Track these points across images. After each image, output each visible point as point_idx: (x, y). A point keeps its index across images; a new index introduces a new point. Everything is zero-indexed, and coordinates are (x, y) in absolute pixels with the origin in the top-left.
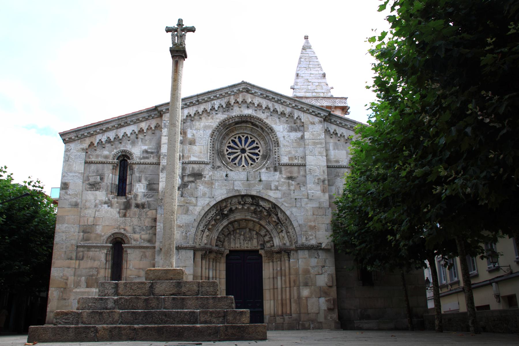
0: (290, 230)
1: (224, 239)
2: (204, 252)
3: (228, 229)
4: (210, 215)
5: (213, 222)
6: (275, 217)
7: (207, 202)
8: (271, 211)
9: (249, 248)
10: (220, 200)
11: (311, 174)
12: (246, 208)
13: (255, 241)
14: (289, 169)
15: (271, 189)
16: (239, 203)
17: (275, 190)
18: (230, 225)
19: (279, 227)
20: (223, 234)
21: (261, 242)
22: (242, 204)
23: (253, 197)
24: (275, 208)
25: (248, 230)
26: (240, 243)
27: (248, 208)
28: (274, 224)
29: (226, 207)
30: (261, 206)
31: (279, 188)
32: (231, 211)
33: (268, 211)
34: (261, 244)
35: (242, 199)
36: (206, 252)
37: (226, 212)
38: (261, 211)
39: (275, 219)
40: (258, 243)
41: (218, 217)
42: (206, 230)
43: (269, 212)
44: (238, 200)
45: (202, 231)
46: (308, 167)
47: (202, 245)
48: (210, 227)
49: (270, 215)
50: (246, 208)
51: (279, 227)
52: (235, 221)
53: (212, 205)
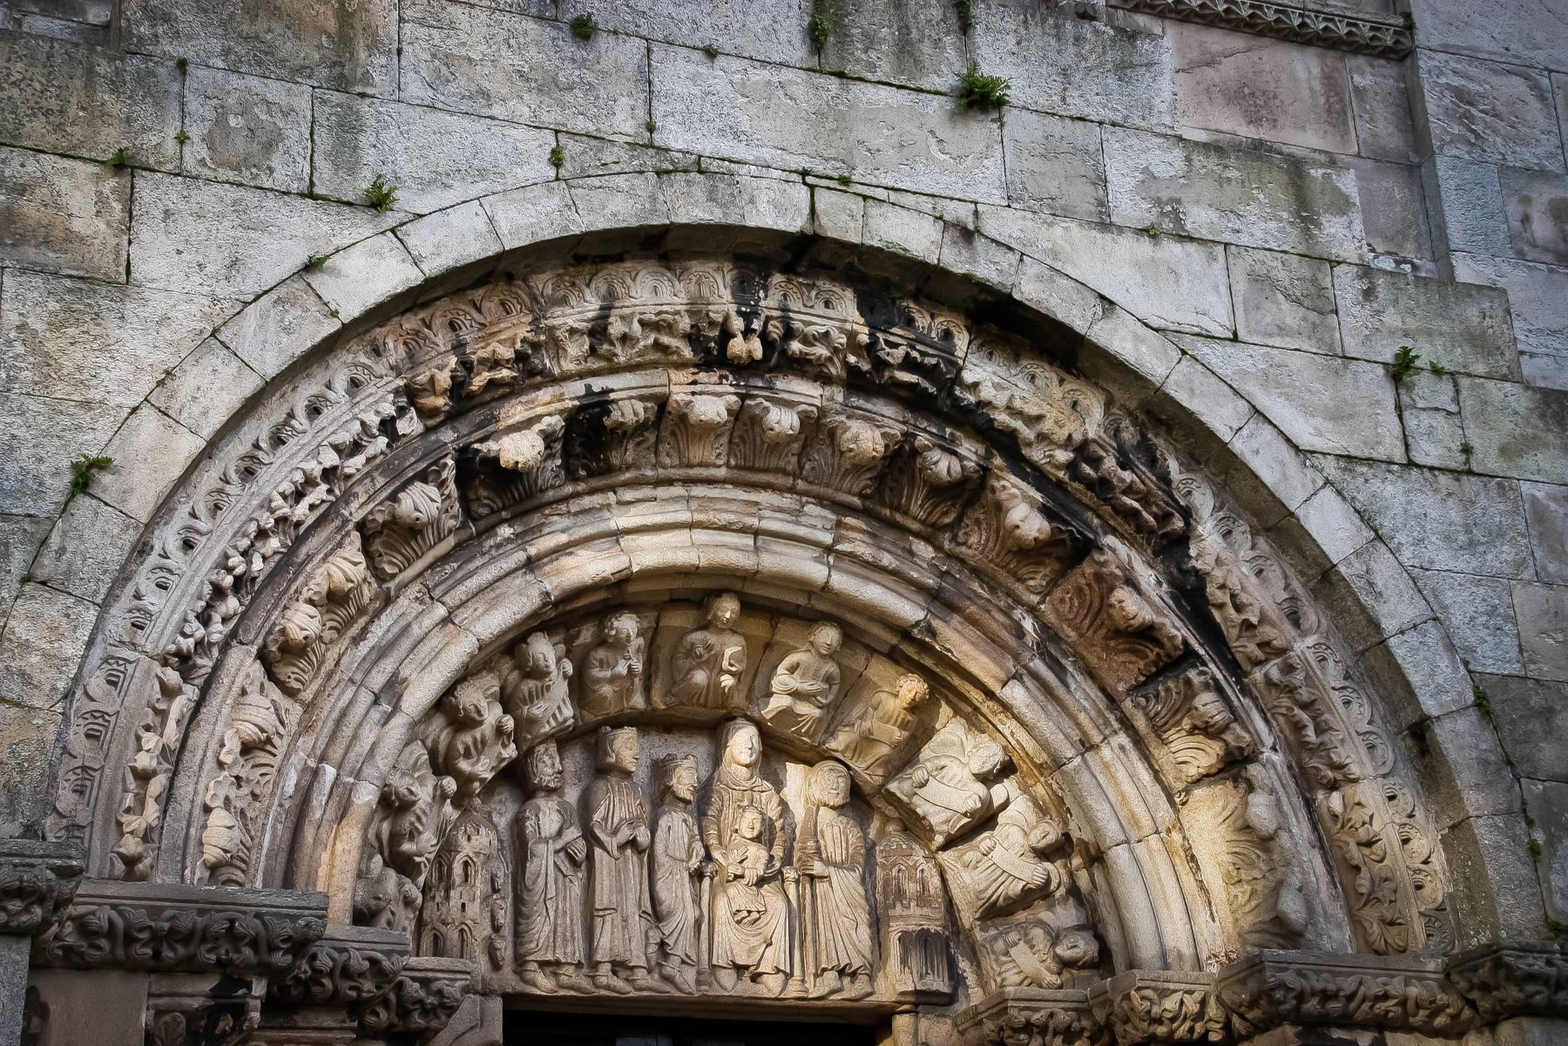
0: (1353, 757)
1: (447, 848)
2: (198, 992)
3: (507, 701)
4: (308, 452)
5: (345, 565)
6: (1147, 576)
7: (277, 257)
8: (1102, 486)
9: (771, 987)
10: (475, 250)
11: (1476, 141)
12: (783, 421)
13: (841, 895)
14: (1228, 70)
15: (1104, 223)
16: (711, 354)
17: (1150, 233)
18: (544, 649)
19: (1207, 703)
20: (441, 764)
21: (910, 918)
22: (743, 369)
23: (885, 281)
24: (1152, 462)
25: (743, 743)
26: (656, 914)
27: (816, 428)
28: (1123, 671)
29: (529, 372)
30: (974, 420)
31: (1199, 218)
32: (589, 442)
33: (1057, 499)
34: (918, 942)
35: (743, 290)
36: (227, 1003)
37: (519, 449)
38: (970, 493)
39: (1144, 597)
40: (877, 924)
41: (422, 501)
42: (243, 665)
43: (1076, 495)
44: (696, 309)
45: (184, 661)
46: (1436, 76)
47: (163, 879)
48: (302, 621)
49: (1083, 548)
50: (783, 421)
51: (1207, 703)
52: (615, 595)
53: (351, 310)
